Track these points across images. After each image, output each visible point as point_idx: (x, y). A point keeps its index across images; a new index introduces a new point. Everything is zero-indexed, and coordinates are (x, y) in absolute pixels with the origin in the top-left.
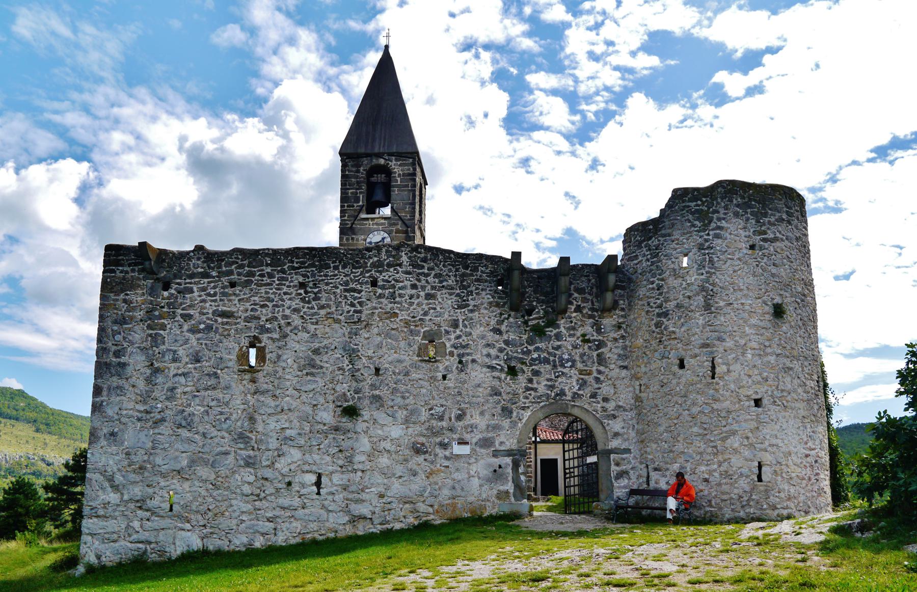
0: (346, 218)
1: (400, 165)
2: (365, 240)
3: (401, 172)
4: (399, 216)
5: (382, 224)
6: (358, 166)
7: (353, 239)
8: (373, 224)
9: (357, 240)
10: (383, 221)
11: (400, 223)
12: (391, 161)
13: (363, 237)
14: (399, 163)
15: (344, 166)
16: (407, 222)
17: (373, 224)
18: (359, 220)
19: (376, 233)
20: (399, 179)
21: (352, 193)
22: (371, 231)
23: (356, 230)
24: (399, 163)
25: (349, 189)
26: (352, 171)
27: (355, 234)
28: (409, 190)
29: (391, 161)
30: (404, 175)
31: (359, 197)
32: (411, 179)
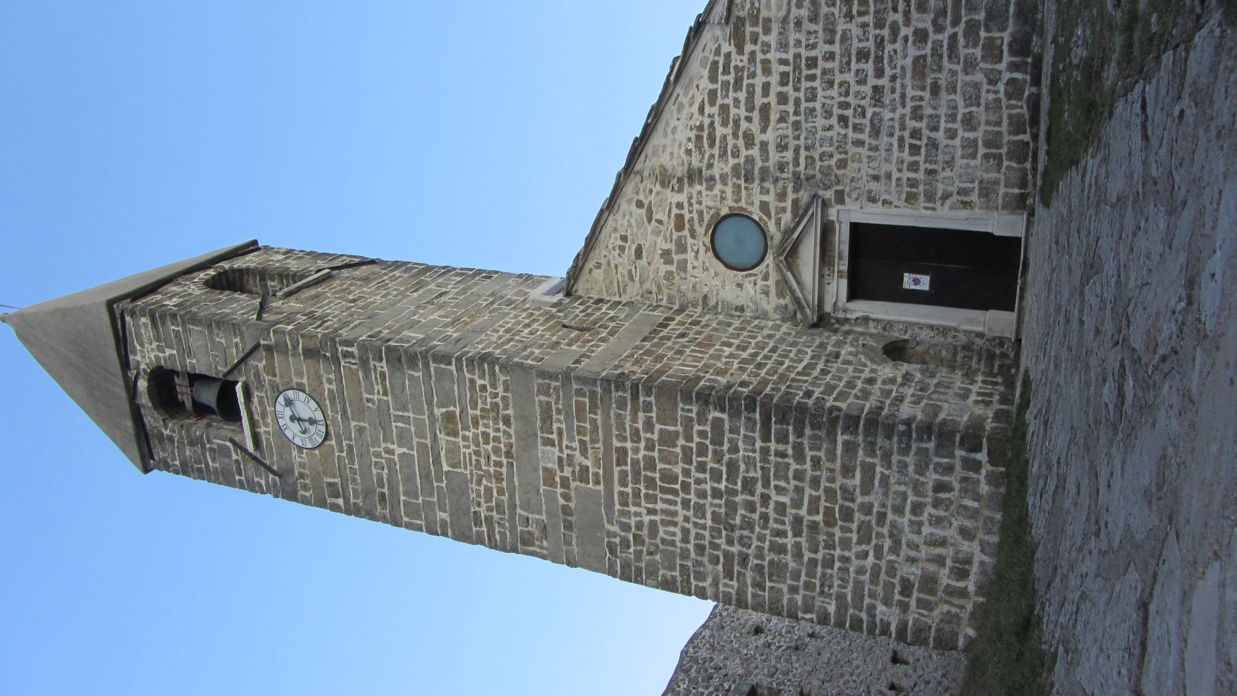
0: (263, 482)
1: (142, 345)
2: (300, 449)
3: (155, 345)
4: (239, 363)
5: (261, 403)
6: (161, 437)
7: (302, 476)
8: (266, 425)
9: (302, 465)
10: (255, 400)
11: (252, 362)
12: (138, 363)
13: (295, 453)
14: (138, 348)
15: (166, 466)
16: (249, 347)
17: (266, 425)
18: (262, 452)
19: (281, 422)
20: (168, 352)
21: (214, 460)
22: (280, 432)
23: (284, 465)
24: (138, 348)
25: (207, 466)
26: (173, 453)
27: (292, 470)
28: (185, 330)
29: (138, 363)
30: (158, 338)
31: (219, 445)
32: (163, 324)
